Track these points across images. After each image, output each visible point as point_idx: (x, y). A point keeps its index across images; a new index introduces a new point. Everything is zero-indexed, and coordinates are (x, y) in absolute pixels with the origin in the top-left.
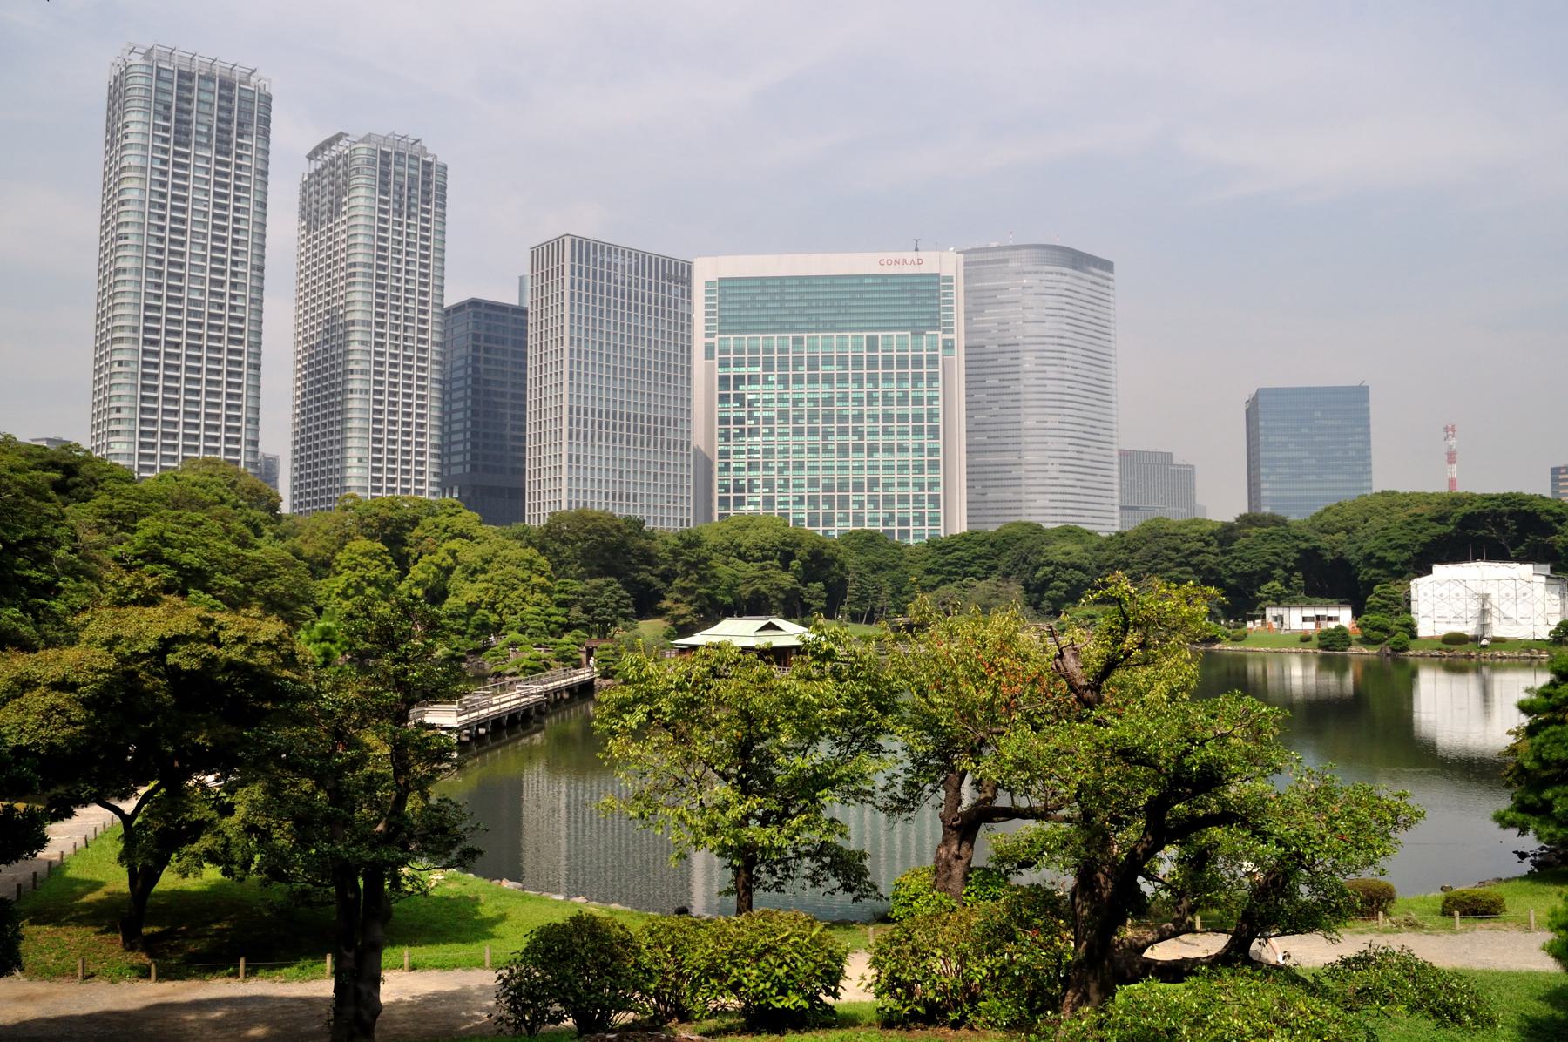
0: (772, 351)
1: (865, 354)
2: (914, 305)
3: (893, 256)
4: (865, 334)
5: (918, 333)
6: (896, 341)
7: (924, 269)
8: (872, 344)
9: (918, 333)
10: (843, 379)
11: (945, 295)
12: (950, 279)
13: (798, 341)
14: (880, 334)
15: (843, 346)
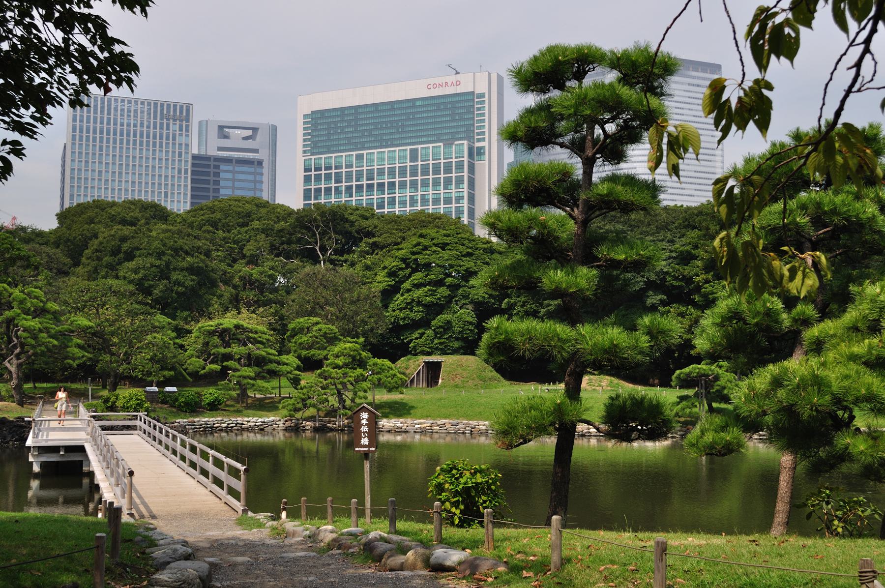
0: (330, 168)
1: (408, 164)
2: (454, 120)
3: (437, 81)
4: (408, 148)
5: (448, 144)
6: (432, 151)
7: (460, 90)
8: (414, 156)
9: (448, 144)
10: (392, 185)
11: (478, 109)
12: (482, 95)
13: (359, 157)
14: (419, 147)
15: (392, 159)
